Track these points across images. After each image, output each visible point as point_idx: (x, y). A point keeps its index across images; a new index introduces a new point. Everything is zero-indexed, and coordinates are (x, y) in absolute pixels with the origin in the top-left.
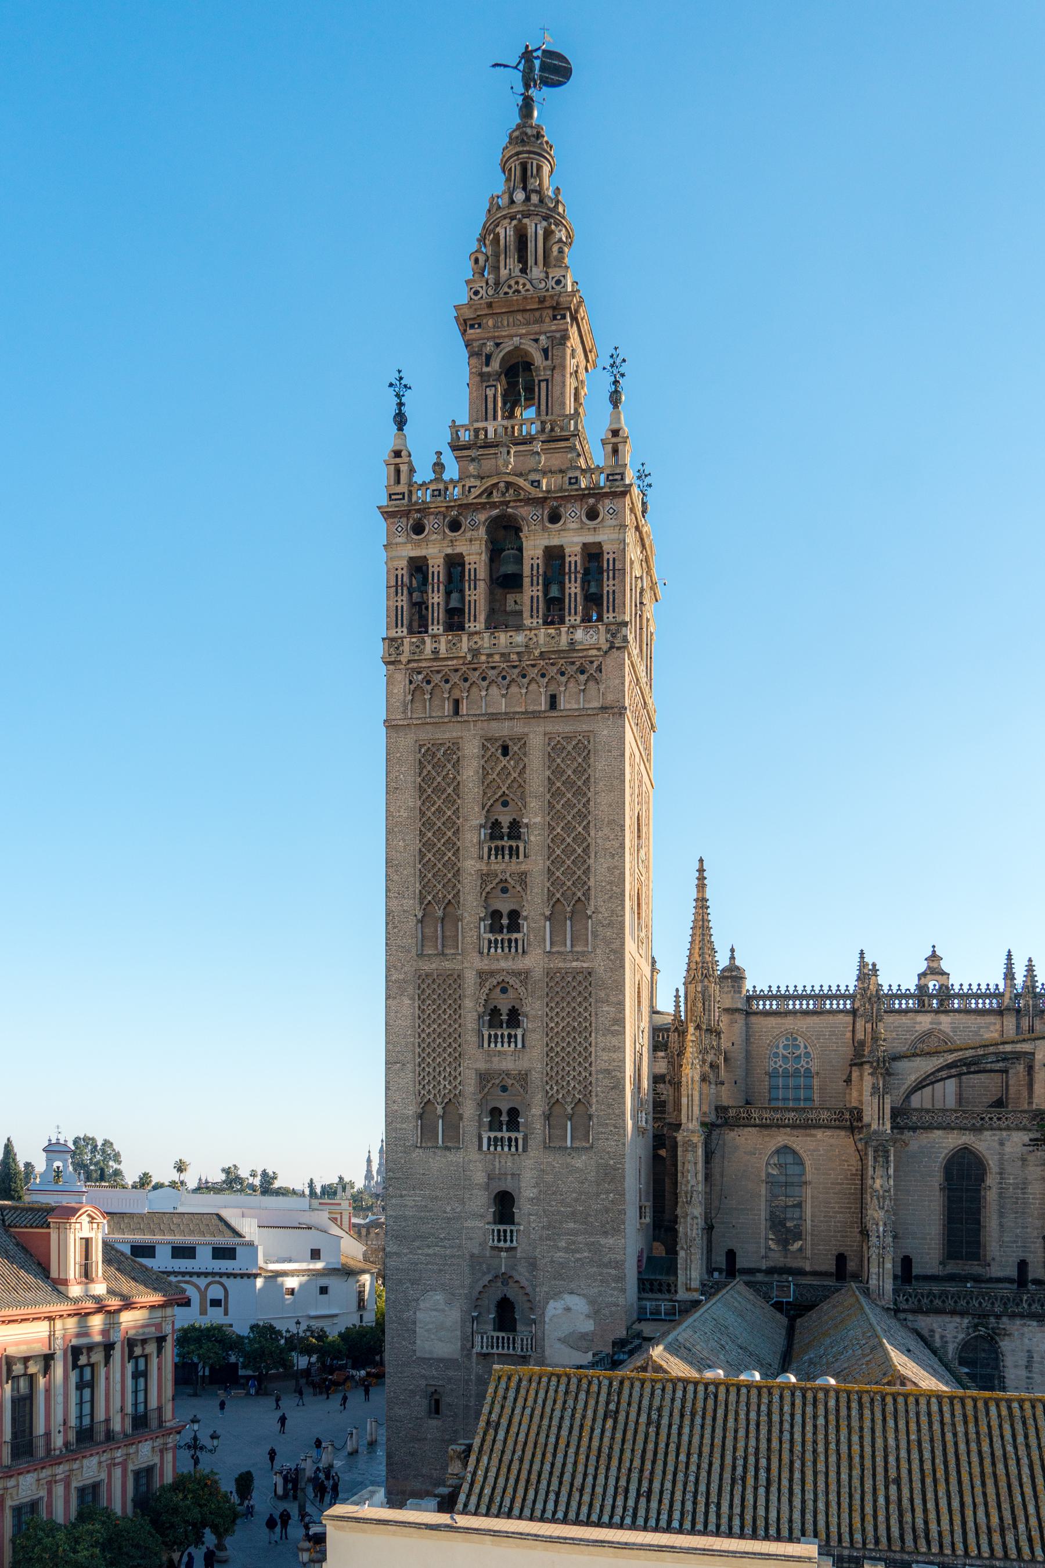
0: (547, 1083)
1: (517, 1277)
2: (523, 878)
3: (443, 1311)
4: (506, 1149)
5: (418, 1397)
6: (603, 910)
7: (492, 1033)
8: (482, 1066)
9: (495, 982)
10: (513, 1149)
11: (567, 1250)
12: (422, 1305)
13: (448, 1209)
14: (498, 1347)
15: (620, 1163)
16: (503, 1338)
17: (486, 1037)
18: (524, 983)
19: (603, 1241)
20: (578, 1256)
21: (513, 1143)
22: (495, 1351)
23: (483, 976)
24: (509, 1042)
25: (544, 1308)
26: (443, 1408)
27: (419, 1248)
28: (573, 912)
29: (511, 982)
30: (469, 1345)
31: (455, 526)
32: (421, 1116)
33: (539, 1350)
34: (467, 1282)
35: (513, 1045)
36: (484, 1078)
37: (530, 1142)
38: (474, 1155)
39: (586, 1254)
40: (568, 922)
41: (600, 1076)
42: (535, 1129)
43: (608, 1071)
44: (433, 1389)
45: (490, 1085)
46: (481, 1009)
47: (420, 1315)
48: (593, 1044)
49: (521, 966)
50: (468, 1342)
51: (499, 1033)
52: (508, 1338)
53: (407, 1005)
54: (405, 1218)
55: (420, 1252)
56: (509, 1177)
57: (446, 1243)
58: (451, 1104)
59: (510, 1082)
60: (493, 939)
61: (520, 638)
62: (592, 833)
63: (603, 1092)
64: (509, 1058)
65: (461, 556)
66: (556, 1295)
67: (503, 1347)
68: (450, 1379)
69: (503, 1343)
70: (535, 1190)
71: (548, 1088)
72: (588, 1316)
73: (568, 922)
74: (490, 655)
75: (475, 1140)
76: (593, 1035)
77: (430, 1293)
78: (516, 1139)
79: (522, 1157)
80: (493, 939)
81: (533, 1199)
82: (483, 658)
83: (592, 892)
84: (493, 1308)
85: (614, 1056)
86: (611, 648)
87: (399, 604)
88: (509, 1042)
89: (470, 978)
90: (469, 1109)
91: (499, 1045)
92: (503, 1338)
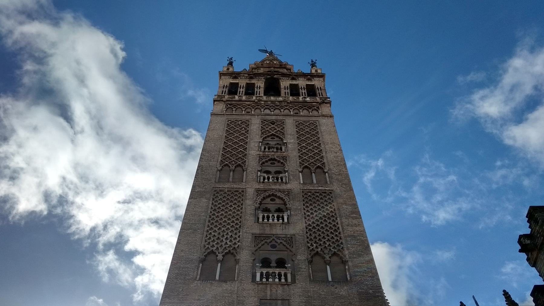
0: (308, 243)
2: (285, 158)
4: (277, 280)
6: (335, 169)
7: (266, 215)
8: (257, 231)
9: (267, 194)
10: (283, 280)
15: (379, 292)
17: (261, 217)
18: (288, 195)
21: (283, 277)
23: (258, 190)
24: (278, 220)
28: (315, 170)
29: (278, 195)
31: (251, 78)
32: (203, 261)
35: (281, 221)
36: (259, 239)
37: (297, 277)
40: (313, 174)
41: (349, 239)
42: (302, 268)
43: (353, 237)
45: (263, 243)
46: (258, 205)
48: (339, 223)
49: (285, 188)
51: (271, 215)
53: (205, 203)
56: (280, 302)
58: (231, 253)
59: (279, 241)
60: (266, 176)
61: (280, 99)
62: (323, 146)
63: (352, 247)
64: (279, 228)
65: (254, 84)
71: (309, 245)
73: (313, 174)
74: (265, 101)
75: (250, 276)
76: (338, 219)
78: (286, 275)
79: (291, 287)
80: (266, 176)
82: (263, 102)
83: (326, 164)
85: (357, 229)
86: (323, 103)
87: (224, 90)
88: (278, 220)
89: (250, 192)
90: (245, 256)
91: (271, 221)
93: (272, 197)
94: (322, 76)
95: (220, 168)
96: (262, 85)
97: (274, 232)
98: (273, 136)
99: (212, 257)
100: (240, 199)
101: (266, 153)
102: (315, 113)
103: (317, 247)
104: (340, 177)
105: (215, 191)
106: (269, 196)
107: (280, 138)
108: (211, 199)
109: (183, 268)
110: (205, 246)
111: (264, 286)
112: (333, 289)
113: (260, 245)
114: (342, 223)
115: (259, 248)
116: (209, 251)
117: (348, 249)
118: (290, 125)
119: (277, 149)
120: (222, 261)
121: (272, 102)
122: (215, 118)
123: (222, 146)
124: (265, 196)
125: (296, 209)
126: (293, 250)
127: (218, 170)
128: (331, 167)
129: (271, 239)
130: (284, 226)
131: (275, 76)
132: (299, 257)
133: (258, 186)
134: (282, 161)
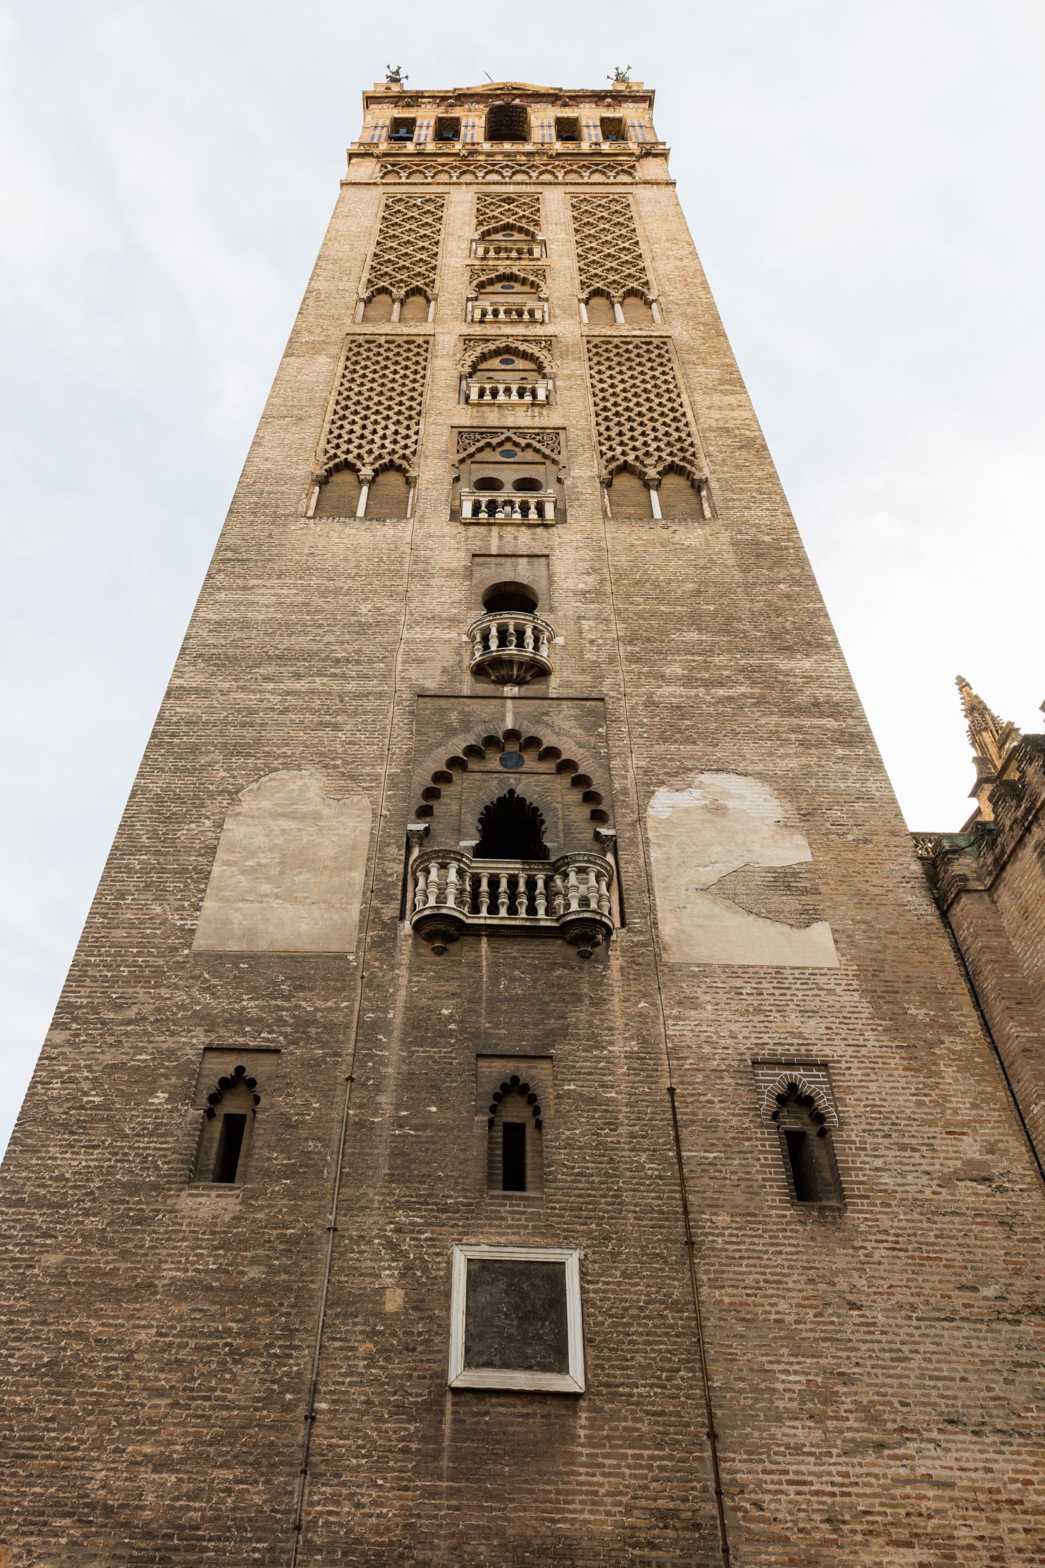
0: (601, 444)
1: (549, 740)
3: (317, 816)
5: (162, 1096)
9: (493, 347)
11: (688, 681)
12: (248, 803)
13: (365, 608)
14: (493, 910)
16: (513, 882)
19: (784, 664)
20: (722, 692)
22: (483, 918)
23: (468, 340)
25: (642, 808)
26: (261, 1148)
27: (268, 679)
30: (390, 911)
32: (323, 482)
33: (636, 922)
34: (400, 748)
35: (528, 399)
38: (439, 524)
39: (743, 689)
40: (617, 306)
44: (226, 1066)
47: (235, 830)
48: (686, 403)
49: (541, 333)
50: (386, 894)
52: (531, 884)
54: (245, 625)
55: (271, 686)
57: (352, 670)
61: (528, 147)
66: (678, 774)
67: (513, 910)
68: (303, 1023)
69: (513, 896)
70: (591, 580)
72: (782, 825)
74: (490, 154)
77: (282, 774)
81: (584, 593)
84: (471, 821)
90: (432, 471)
92: (513, 882)
93: (506, 356)
94: (647, 98)
95: (365, 296)
96: (482, 122)
97: (510, 422)
98: (508, 229)
99: (345, 478)
100: (420, 359)
101: (491, 263)
102: (624, 178)
103: (624, 453)
104: (690, 310)
105: (353, 342)
106: (497, 353)
107: (527, 233)
108: (343, 358)
109: (269, 493)
110: (326, 452)
111: (481, 530)
112: (665, 534)
113: (472, 449)
114: (692, 404)
115: (471, 455)
116: (337, 460)
117: (708, 455)
118: (555, 207)
119: (520, 252)
120: (372, 482)
121: (507, 154)
122: (352, 190)
123: (372, 249)
124: (486, 351)
125: (569, 377)
126: (562, 459)
127: (361, 300)
128: (667, 288)
129: (503, 437)
130: (536, 410)
131: (517, 101)
132: (575, 472)
133: (466, 330)
134: (532, 278)
